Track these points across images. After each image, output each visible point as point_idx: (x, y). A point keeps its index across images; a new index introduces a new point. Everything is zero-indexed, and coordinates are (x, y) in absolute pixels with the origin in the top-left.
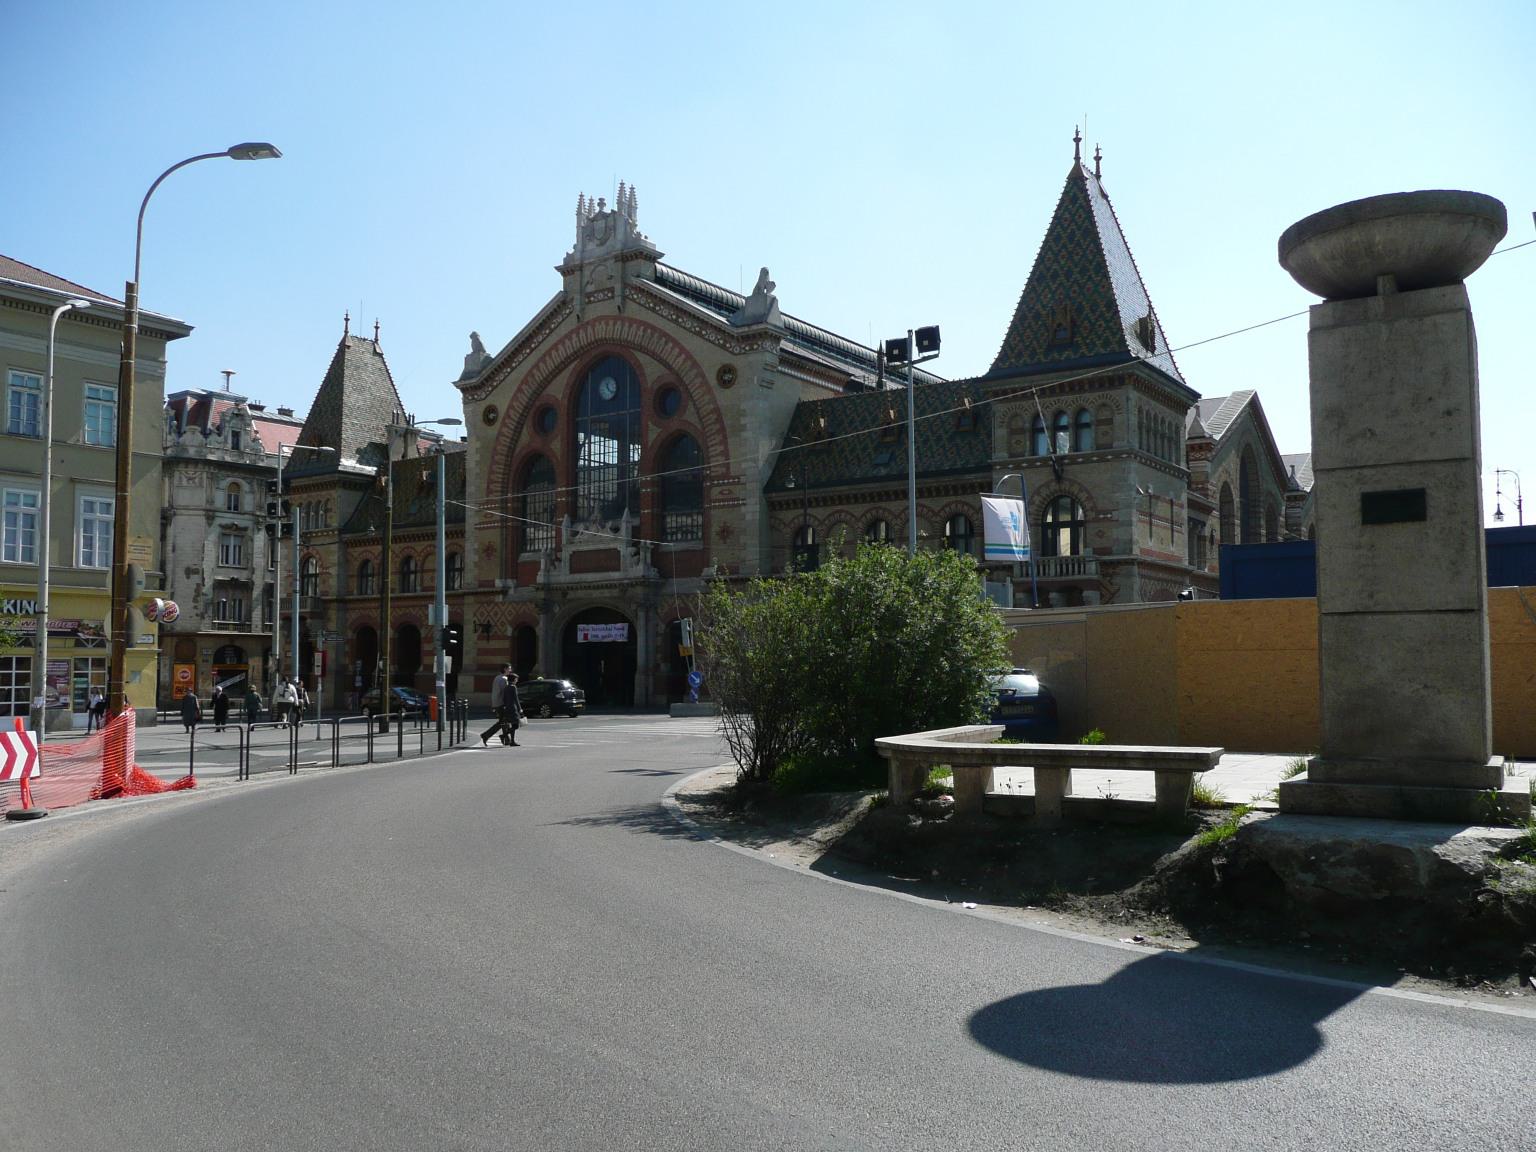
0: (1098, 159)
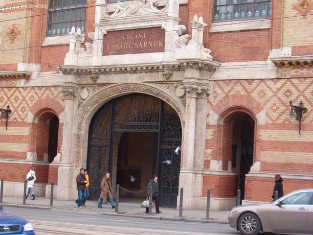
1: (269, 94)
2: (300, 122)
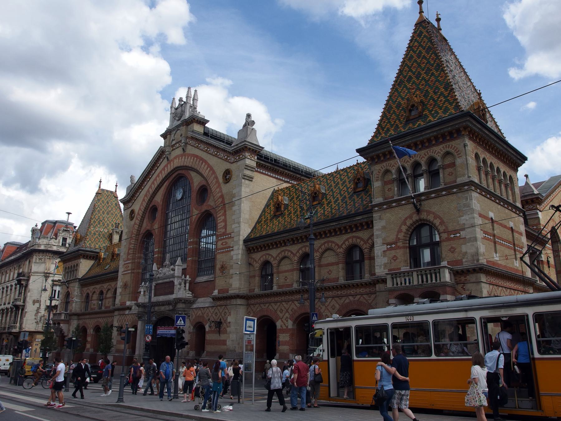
0: (438, 20)
1: (210, 314)
2: (220, 329)
